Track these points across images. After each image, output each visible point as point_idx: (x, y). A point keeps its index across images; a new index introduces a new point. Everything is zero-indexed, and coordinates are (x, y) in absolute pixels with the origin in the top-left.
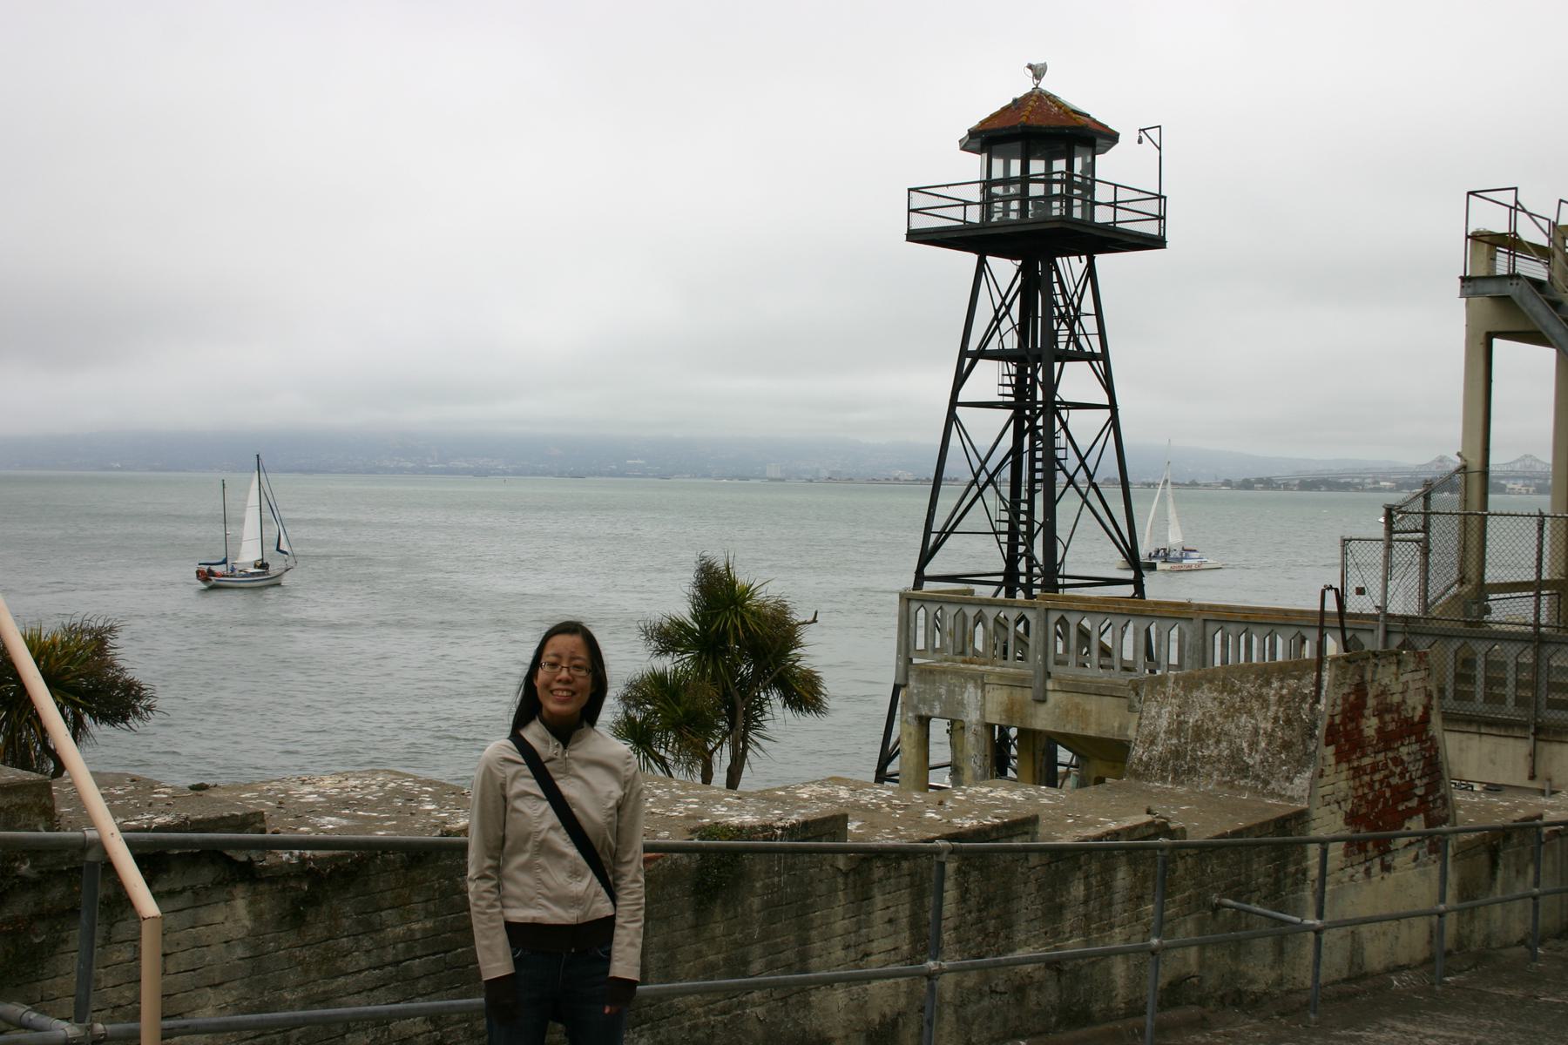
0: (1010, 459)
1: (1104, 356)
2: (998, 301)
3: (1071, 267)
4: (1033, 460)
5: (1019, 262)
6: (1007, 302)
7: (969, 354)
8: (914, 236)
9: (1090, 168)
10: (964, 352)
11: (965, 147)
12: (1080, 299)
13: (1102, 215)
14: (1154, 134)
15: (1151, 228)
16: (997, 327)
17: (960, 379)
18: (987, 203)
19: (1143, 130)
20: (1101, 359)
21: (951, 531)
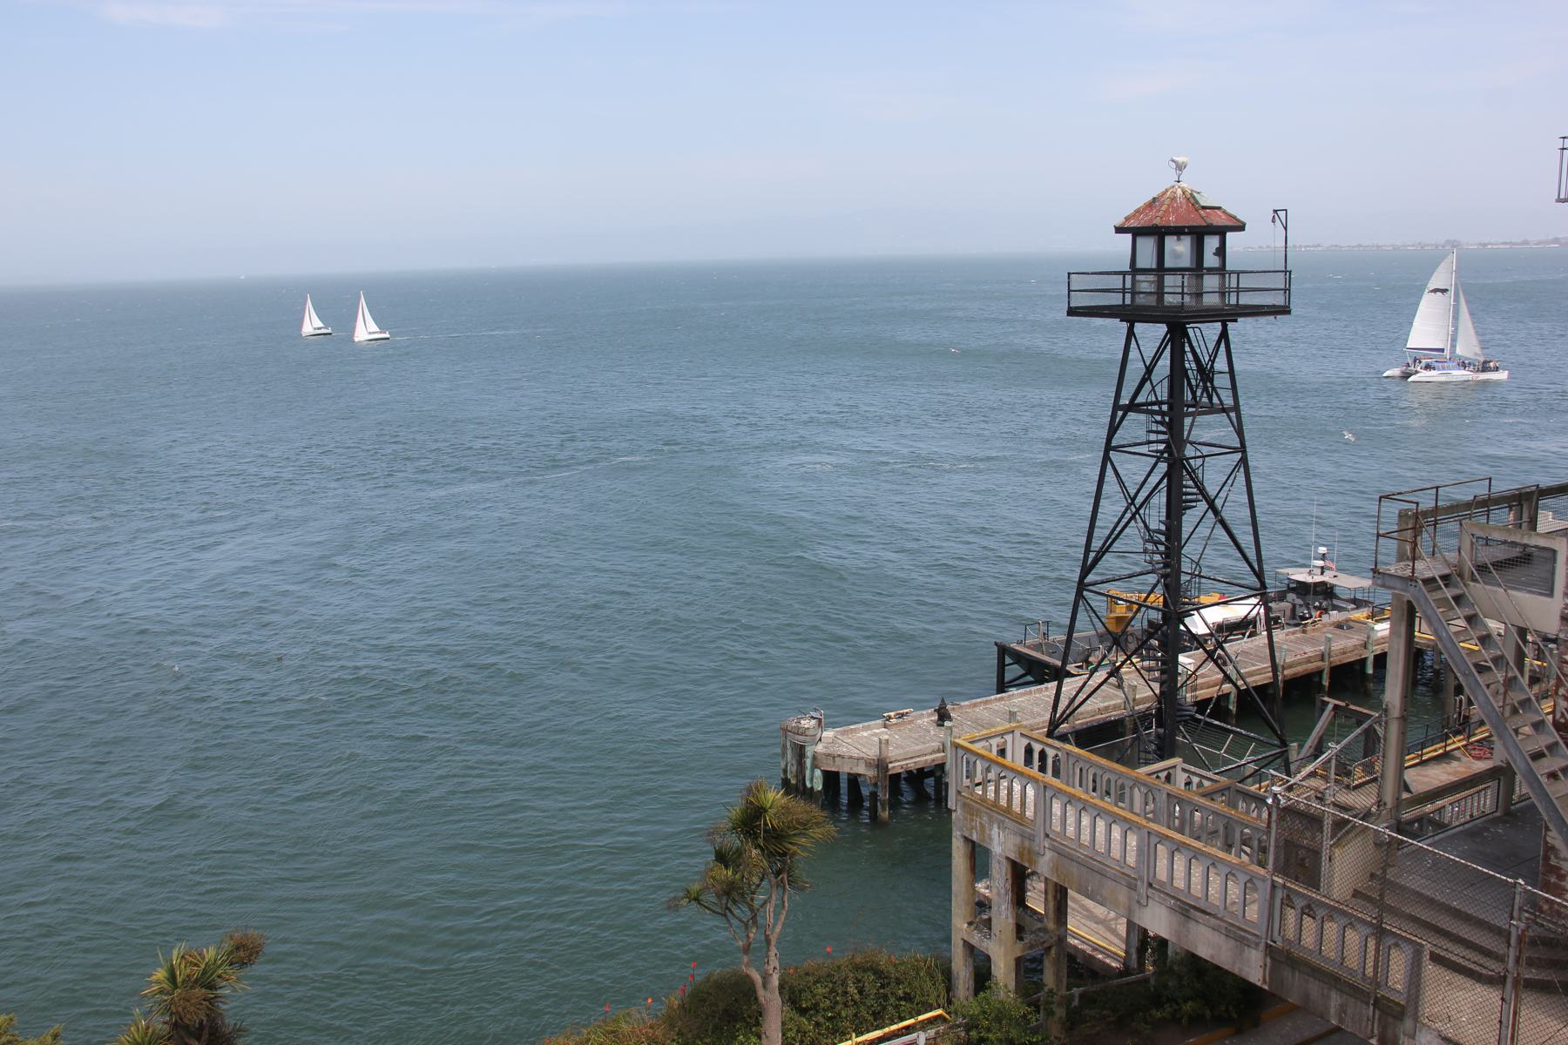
8: (1072, 312)
9: (1221, 252)
11: (1119, 230)
15: (1278, 300)
17: (1113, 429)
21: (1107, 551)
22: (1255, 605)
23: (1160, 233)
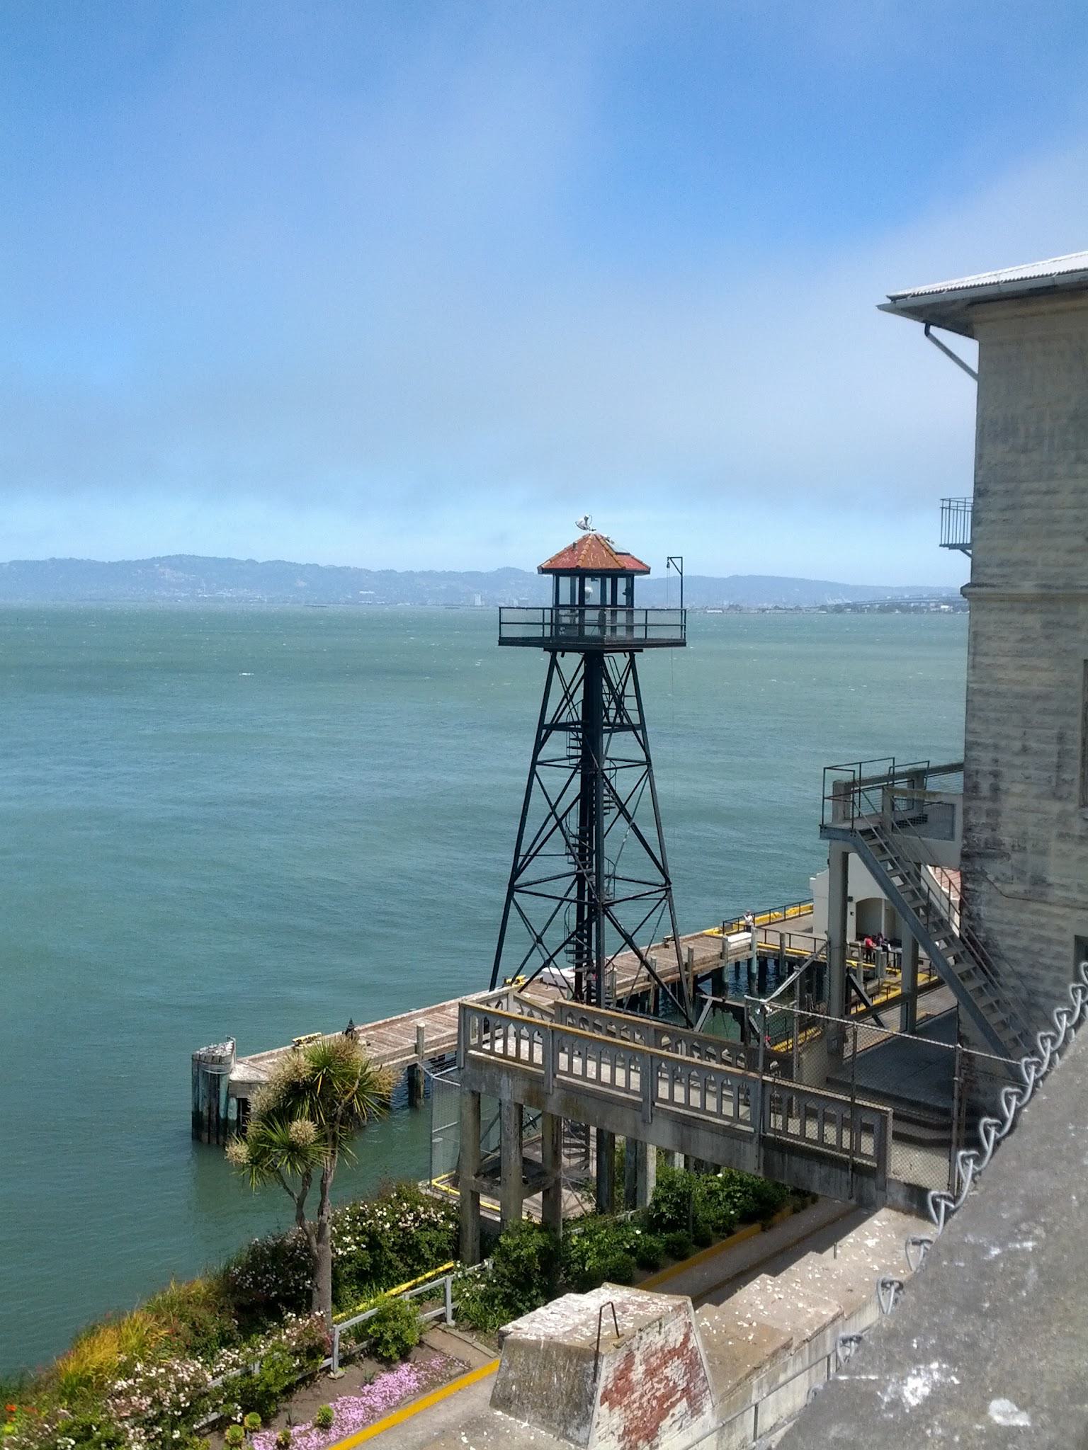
1: (642, 726)
7: (546, 727)
8: (503, 642)
9: (630, 592)
10: (541, 725)
11: (543, 571)
15: (675, 634)
17: (539, 745)
21: (535, 854)
22: (662, 900)
23: (580, 574)
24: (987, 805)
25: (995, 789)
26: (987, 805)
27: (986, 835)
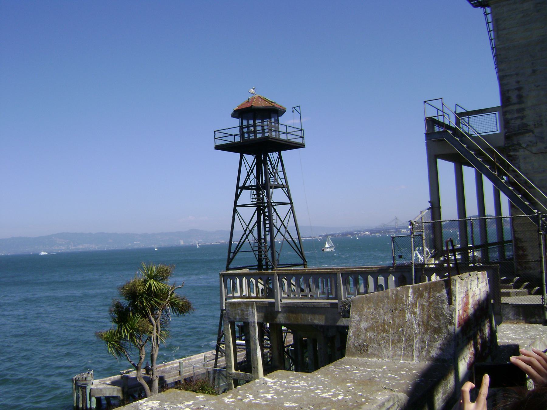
0: (257, 224)
2: (248, 169)
3: (274, 156)
4: (265, 224)
5: (255, 156)
6: (252, 169)
8: (218, 147)
10: (238, 188)
12: (277, 166)
13: (283, 137)
14: (298, 109)
15: (300, 141)
16: (249, 178)
17: (237, 197)
18: (242, 134)
19: (294, 108)
20: (285, 187)
24: (515, 107)
25: (520, 97)
26: (515, 107)
27: (518, 122)
